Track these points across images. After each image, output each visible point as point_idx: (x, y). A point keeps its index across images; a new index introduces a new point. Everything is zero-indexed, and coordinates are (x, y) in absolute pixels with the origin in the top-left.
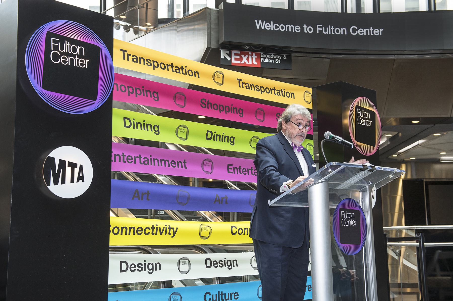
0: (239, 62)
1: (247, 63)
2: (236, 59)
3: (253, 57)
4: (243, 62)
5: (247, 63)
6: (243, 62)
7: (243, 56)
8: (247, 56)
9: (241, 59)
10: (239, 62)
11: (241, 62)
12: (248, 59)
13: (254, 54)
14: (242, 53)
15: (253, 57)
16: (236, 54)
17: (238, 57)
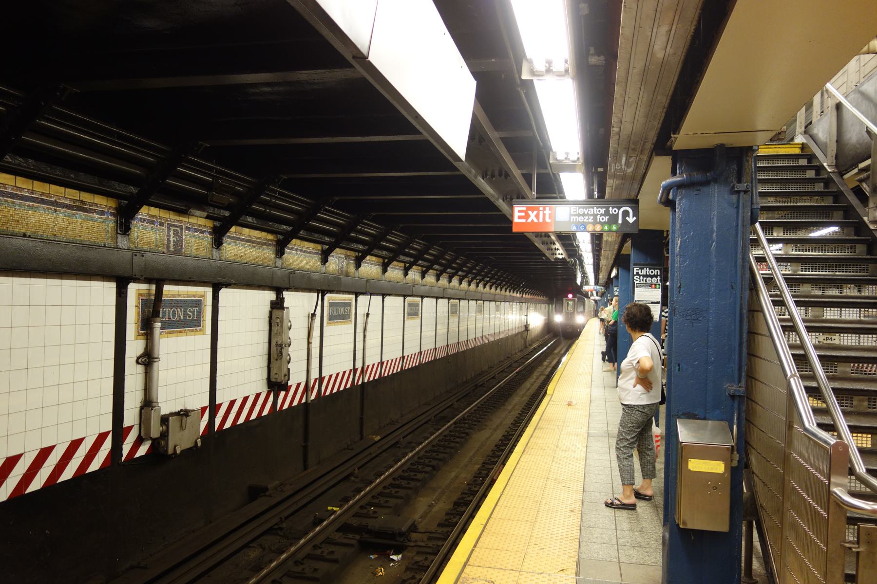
0: (524, 221)
1: (535, 220)
2: (520, 217)
3: (545, 212)
4: (529, 220)
5: (535, 220)
6: (529, 220)
7: (530, 212)
8: (535, 212)
9: (527, 216)
10: (524, 221)
11: (526, 221)
12: (537, 216)
13: (547, 209)
14: (528, 209)
15: (545, 212)
16: (519, 211)
17: (523, 214)
